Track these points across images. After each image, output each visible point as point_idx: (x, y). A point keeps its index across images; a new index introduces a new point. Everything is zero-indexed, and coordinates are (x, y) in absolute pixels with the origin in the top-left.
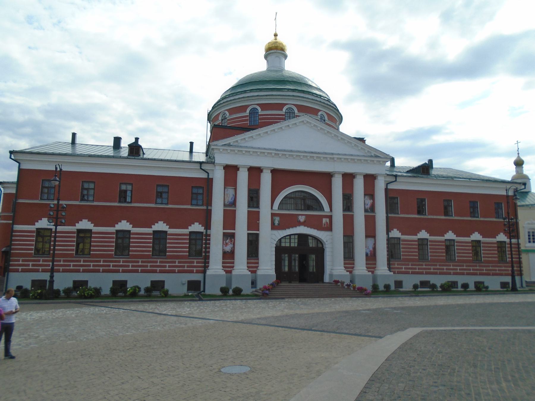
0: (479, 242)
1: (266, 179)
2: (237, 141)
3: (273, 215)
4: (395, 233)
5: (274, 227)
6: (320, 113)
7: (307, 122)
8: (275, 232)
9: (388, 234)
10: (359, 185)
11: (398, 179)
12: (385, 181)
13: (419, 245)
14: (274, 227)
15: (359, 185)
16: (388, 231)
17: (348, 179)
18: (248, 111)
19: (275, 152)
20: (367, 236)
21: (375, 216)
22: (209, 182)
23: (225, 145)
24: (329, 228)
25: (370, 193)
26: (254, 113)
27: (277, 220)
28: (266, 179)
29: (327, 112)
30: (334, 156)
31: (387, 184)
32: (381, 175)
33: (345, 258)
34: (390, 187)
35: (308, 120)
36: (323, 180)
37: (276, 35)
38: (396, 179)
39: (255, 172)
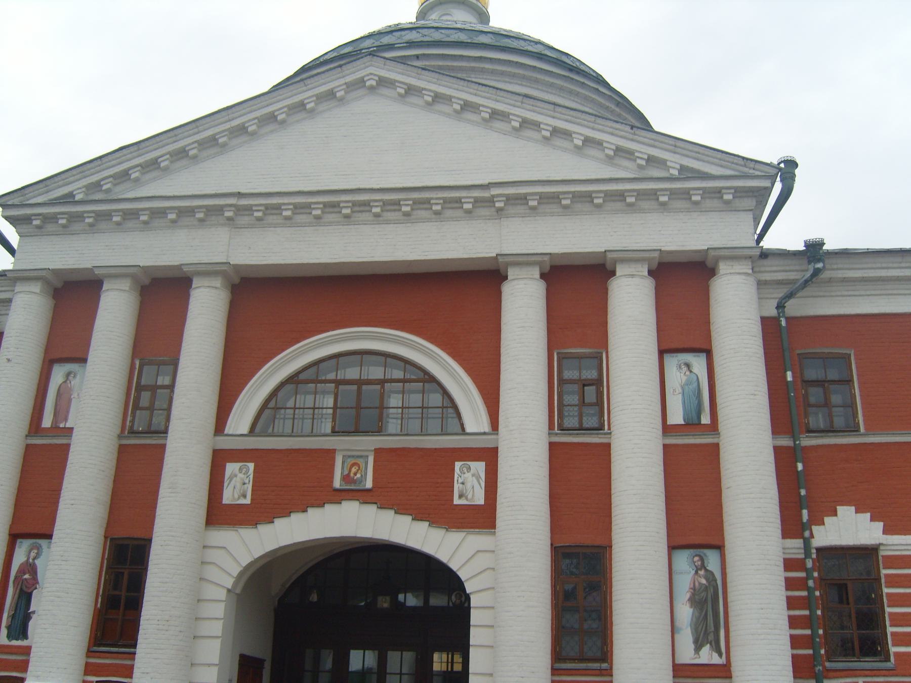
2: (97, 185)
3: (219, 460)
5: (218, 514)
7: (383, 82)
8: (224, 536)
9: (792, 526)
10: (631, 304)
12: (761, 284)
14: (218, 514)
19: (232, 201)
20: (676, 544)
21: (717, 446)
23: (55, 199)
24: (483, 518)
27: (239, 484)
30: (495, 191)
32: (734, 255)
33: (558, 655)
35: (384, 73)
36: (457, 299)
39: (164, 294)
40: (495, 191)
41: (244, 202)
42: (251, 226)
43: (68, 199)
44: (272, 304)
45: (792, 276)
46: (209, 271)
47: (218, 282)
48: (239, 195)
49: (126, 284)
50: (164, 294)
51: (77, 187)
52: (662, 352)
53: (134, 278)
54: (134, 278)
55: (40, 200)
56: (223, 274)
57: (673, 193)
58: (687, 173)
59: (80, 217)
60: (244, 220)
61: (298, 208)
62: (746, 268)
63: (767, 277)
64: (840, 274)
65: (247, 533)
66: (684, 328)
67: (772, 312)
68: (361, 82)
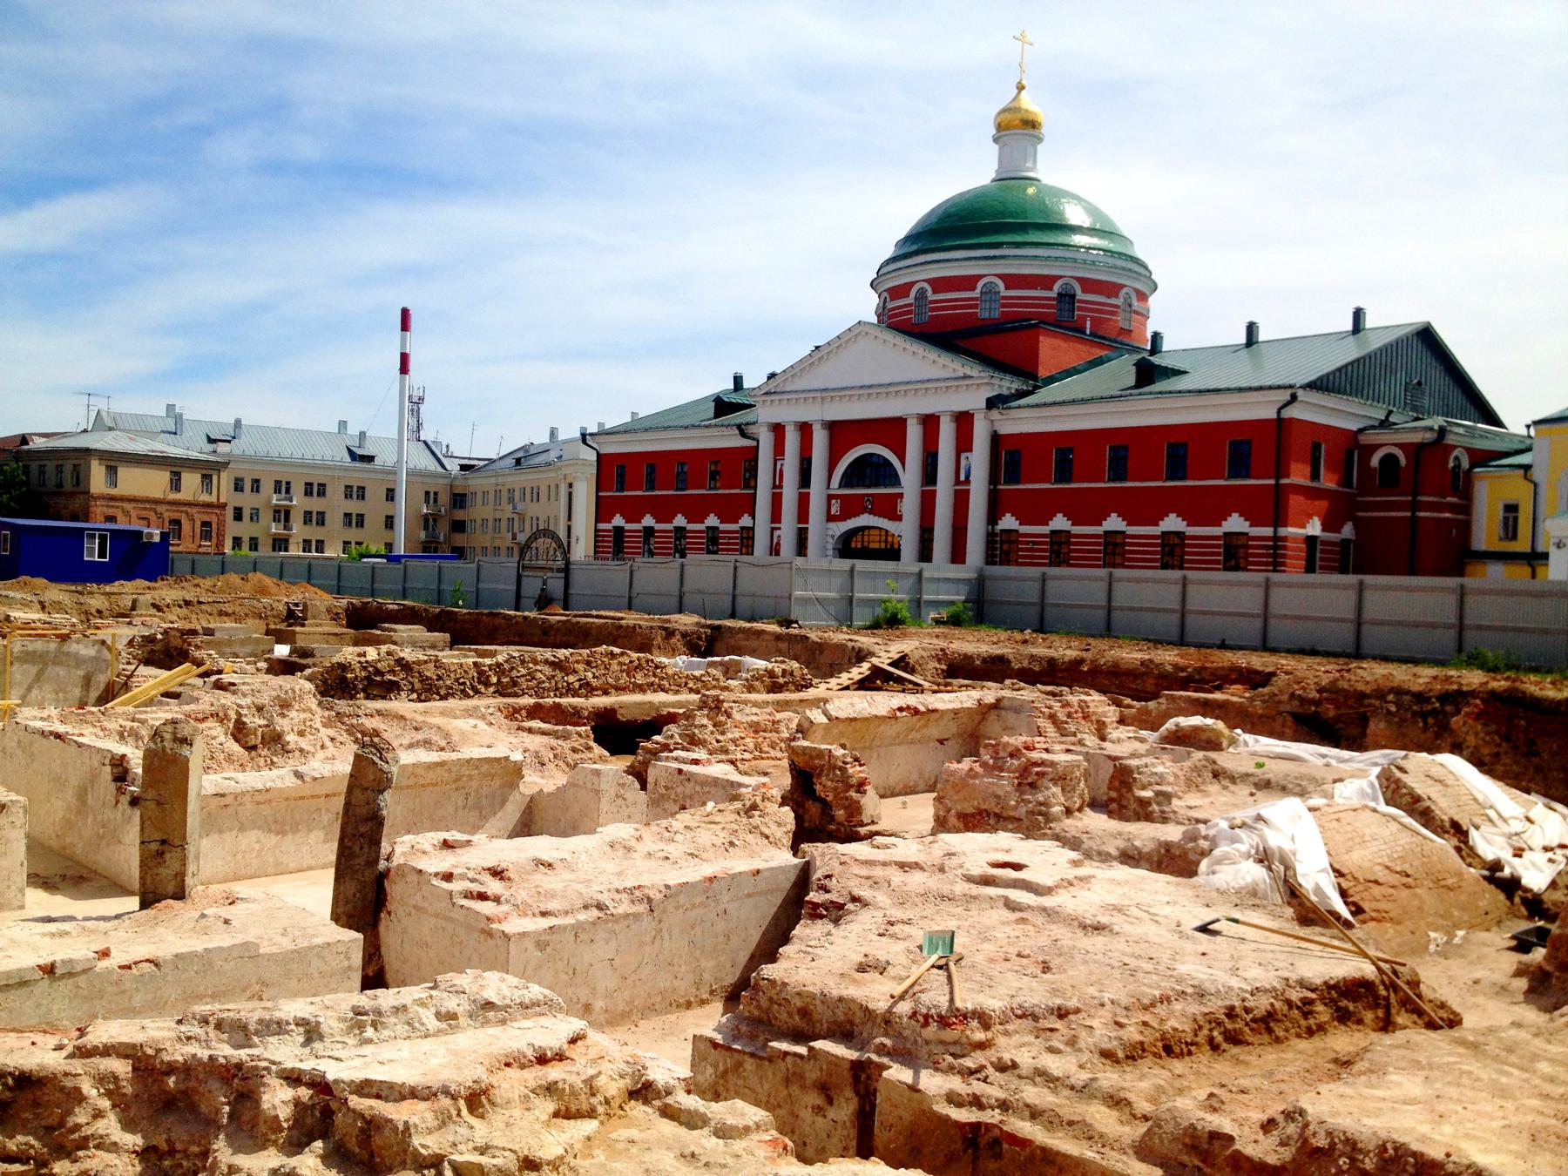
0: (1180, 535)
1: (820, 440)
4: (1008, 522)
6: (980, 285)
8: (832, 525)
10: (947, 432)
13: (1052, 543)
14: (830, 518)
15: (947, 432)
16: (993, 516)
17: (930, 423)
22: (755, 450)
25: (964, 443)
27: (835, 509)
29: (1007, 271)
37: (1021, 88)
39: (805, 429)
44: (843, 433)
65: (840, 524)
66: (964, 443)
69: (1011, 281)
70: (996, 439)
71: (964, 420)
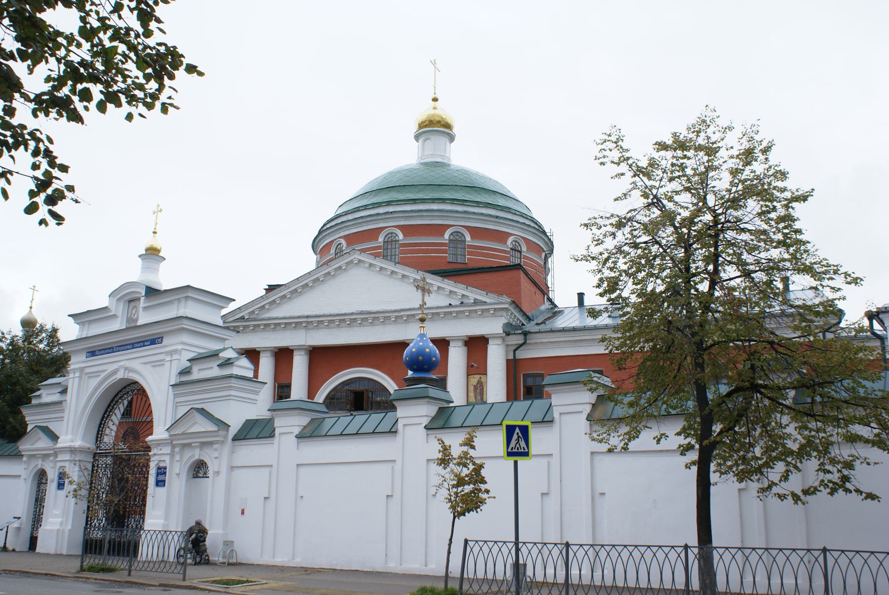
1: (300, 366)
7: (360, 261)
11: (532, 339)
18: (333, 251)
26: (392, 241)
28: (300, 366)
30: (402, 313)
31: (515, 351)
32: (495, 336)
34: (522, 354)
38: (526, 340)
39: (283, 356)
40: (402, 313)
41: (309, 320)
42: (313, 329)
43: (243, 318)
44: (323, 358)
45: (515, 342)
46: (300, 348)
47: (303, 353)
48: (308, 317)
49: (268, 354)
50: (283, 356)
51: (244, 313)
52: (468, 375)
53: (271, 351)
54: (271, 351)
55: (232, 319)
56: (305, 349)
57: (470, 311)
58: (476, 302)
59: (248, 326)
60: (311, 326)
61: (330, 322)
62: (499, 341)
63: (510, 343)
64: (539, 341)
67: (511, 357)
68: (352, 261)
69: (476, 232)
70: (513, 366)
71: (476, 346)
